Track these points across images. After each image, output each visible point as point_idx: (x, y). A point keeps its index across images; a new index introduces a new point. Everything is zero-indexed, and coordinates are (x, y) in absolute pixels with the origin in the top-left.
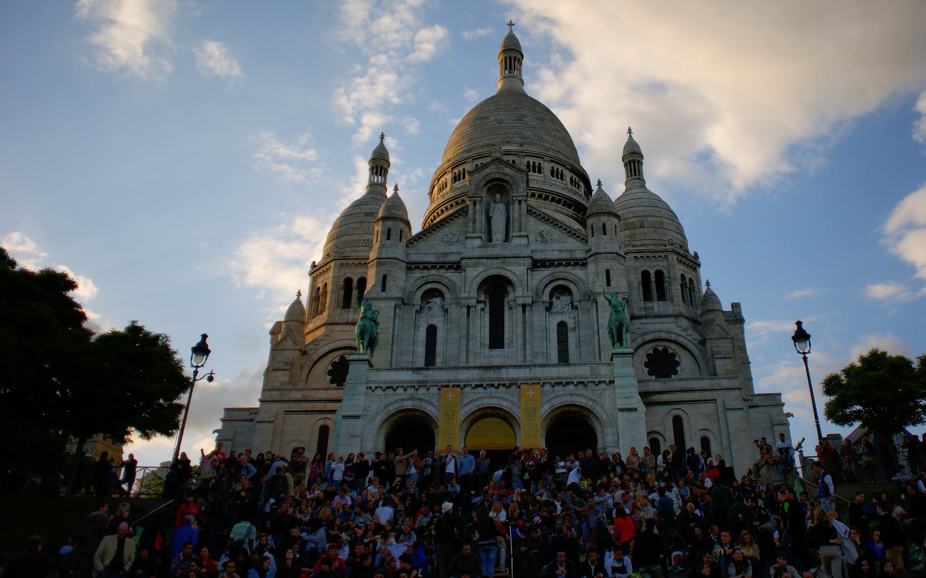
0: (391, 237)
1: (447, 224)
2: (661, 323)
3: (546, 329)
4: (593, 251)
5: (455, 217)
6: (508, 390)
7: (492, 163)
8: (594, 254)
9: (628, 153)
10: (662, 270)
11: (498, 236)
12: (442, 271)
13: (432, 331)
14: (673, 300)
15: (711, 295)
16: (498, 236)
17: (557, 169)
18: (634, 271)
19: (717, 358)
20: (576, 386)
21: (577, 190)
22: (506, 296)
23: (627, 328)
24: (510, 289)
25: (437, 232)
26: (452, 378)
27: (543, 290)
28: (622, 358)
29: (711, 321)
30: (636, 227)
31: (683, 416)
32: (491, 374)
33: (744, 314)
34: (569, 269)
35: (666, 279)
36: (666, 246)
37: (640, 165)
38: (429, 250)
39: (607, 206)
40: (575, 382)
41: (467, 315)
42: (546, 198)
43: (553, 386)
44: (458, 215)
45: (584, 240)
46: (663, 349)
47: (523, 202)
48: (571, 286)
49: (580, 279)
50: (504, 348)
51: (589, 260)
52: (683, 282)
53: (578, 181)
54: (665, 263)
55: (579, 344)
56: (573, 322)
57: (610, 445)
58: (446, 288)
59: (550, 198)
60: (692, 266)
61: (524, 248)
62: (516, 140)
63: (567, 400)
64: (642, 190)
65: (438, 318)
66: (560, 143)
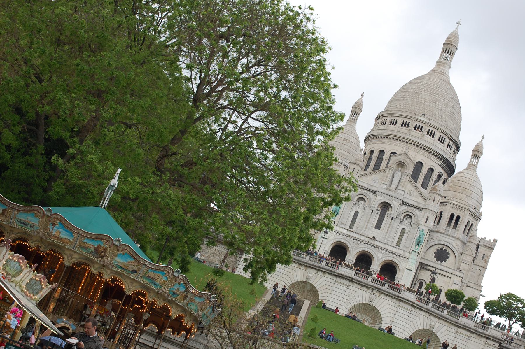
11: (394, 186)
13: (357, 213)
16: (394, 186)
21: (449, 150)
24: (390, 209)
29: (469, 246)
32: (371, 241)
33: (496, 248)
35: (460, 221)
42: (431, 152)
45: (425, 200)
48: (413, 217)
54: (463, 214)
59: (432, 153)
62: (428, 114)
63: (392, 259)
64: (471, 173)
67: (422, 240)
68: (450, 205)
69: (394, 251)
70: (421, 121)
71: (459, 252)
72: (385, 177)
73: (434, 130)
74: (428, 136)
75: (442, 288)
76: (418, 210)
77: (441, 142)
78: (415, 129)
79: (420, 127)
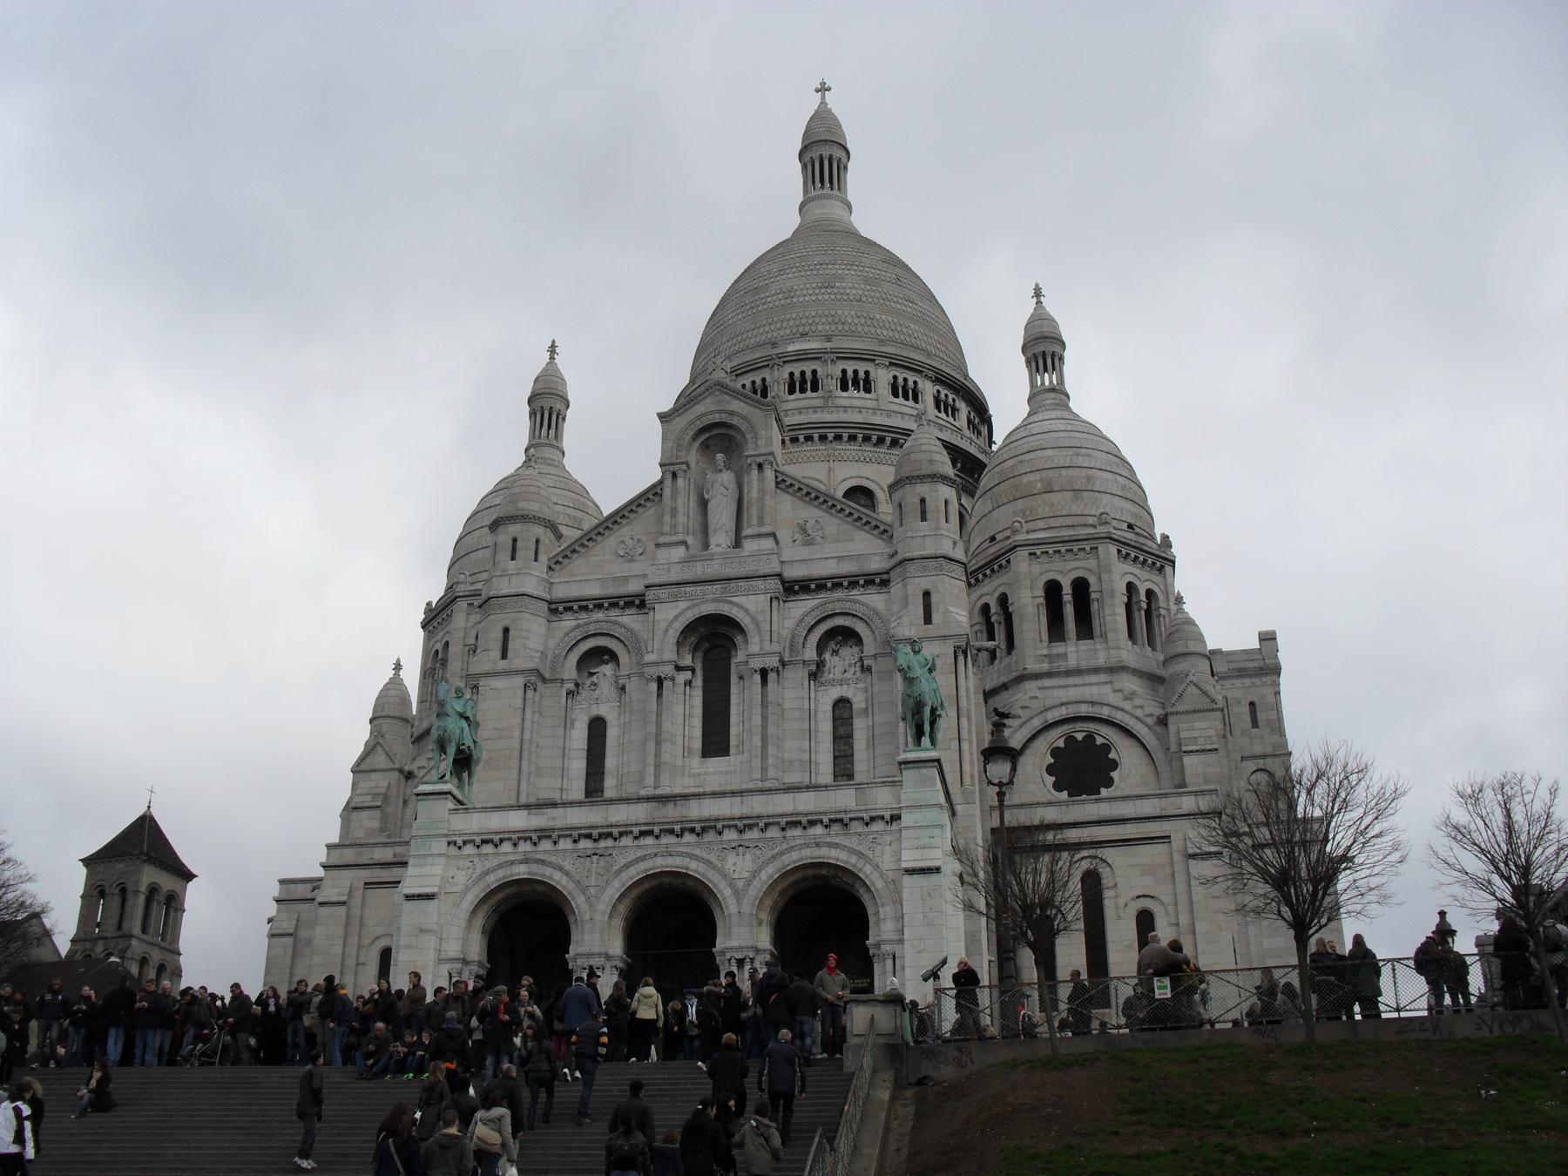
0: (518, 554)
1: (624, 521)
2: (1081, 685)
3: (811, 715)
4: (900, 557)
5: (640, 505)
6: (699, 839)
7: (706, 394)
8: (901, 562)
9: (1032, 337)
10: (1086, 576)
11: (721, 539)
12: (614, 614)
13: (597, 728)
14: (1106, 638)
15: (1183, 623)
16: (721, 539)
17: (905, 380)
18: (1028, 582)
19: (1185, 752)
20: (826, 827)
21: (951, 419)
22: (733, 653)
23: (933, 710)
24: (739, 639)
25: (608, 537)
26: (599, 820)
27: (805, 638)
28: (917, 770)
30: (1035, 492)
31: (1104, 872)
32: (671, 812)
34: (855, 593)
35: (1093, 596)
36: (1094, 527)
37: (1057, 362)
38: (592, 574)
39: (931, 462)
40: (826, 820)
41: (658, 695)
42: (881, 441)
43: (783, 829)
44: (645, 501)
45: (885, 533)
46: (1084, 738)
47: (765, 466)
48: (860, 628)
49: (876, 613)
50: (728, 755)
51: (893, 574)
52: (1134, 600)
53: (954, 400)
54: (1092, 563)
55: (872, 741)
56: (863, 698)
57: (886, 938)
58: (622, 646)
59: (888, 440)
60: (1154, 564)
61: (765, 557)
62: (820, 328)
65: (611, 704)
66: (912, 326)
67: (925, 687)
68: (1023, 553)
69: (801, 808)
70: (802, 357)
71: (1150, 721)
72: (667, 518)
73: (862, 368)
74: (852, 392)
75: (1148, 904)
76: (872, 589)
77: (906, 398)
78: (792, 391)
79: (809, 375)
